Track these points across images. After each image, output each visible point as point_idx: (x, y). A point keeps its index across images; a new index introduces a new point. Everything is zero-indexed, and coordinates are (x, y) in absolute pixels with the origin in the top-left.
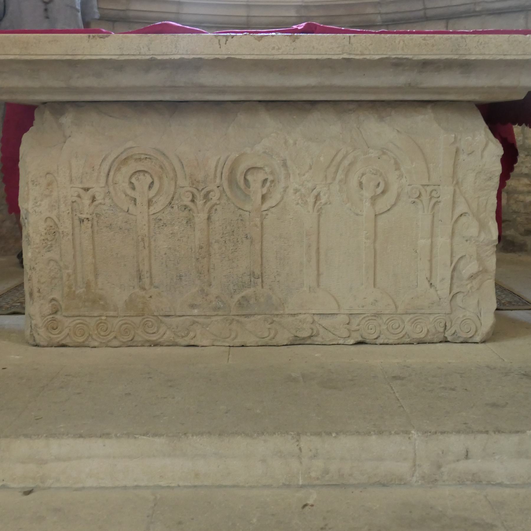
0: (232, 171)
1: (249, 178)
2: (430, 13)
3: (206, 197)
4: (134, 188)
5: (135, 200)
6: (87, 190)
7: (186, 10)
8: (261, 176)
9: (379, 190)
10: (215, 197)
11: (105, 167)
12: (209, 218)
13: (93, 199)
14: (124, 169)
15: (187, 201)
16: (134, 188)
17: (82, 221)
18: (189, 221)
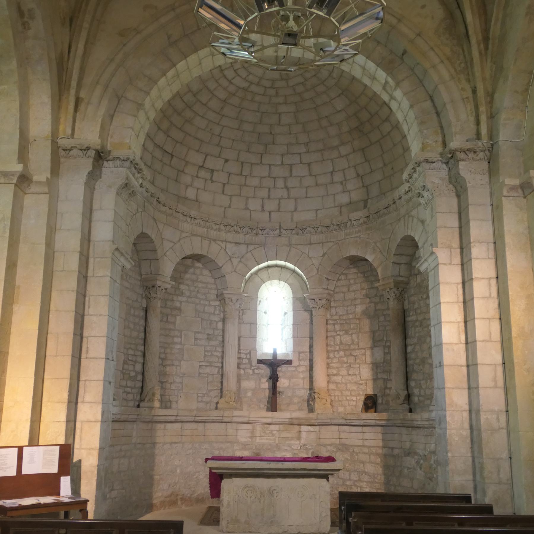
0: (269, 490)
1: (273, 492)
2: (333, 423)
3: (264, 496)
4: (247, 494)
5: (247, 497)
6: (237, 494)
7: (251, 419)
8: (276, 492)
9: (302, 495)
10: (265, 496)
11: (242, 488)
12: (264, 501)
13: (238, 496)
14: (246, 489)
15: (259, 497)
16: (247, 494)
17: (235, 501)
18: (260, 502)
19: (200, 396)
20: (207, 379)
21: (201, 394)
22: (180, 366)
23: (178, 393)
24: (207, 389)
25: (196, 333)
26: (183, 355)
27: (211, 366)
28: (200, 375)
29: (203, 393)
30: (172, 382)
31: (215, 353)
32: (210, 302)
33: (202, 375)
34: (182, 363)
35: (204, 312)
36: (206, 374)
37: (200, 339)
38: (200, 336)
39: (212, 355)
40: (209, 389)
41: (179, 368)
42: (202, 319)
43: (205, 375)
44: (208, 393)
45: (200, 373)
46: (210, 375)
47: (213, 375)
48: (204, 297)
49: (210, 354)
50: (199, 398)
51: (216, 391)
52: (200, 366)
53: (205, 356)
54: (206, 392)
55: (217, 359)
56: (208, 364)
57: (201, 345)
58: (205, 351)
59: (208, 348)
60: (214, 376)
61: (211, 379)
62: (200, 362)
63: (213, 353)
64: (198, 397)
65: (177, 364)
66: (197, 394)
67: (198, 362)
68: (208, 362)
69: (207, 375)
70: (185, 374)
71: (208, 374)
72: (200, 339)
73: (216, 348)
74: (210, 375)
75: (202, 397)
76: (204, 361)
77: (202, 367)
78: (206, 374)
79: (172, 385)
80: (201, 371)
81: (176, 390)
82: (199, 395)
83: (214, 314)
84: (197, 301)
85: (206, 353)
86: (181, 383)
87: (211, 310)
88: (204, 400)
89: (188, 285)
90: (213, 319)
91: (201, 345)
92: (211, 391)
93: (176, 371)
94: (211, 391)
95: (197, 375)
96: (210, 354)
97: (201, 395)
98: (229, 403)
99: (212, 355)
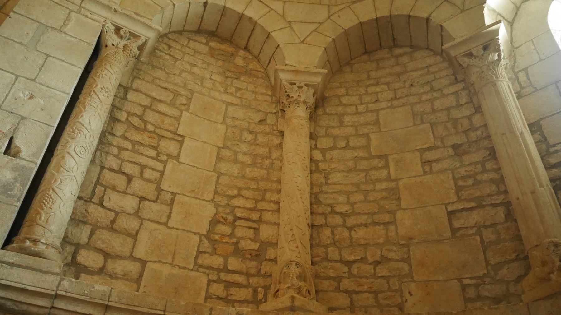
19: (470, 285)
20: (478, 238)
21: (471, 278)
22: (394, 223)
23: (400, 285)
24: (487, 262)
25: (423, 151)
26: (399, 199)
27: (479, 206)
28: (458, 234)
29: (474, 275)
30: (379, 259)
31: (485, 177)
32: (442, 91)
33: (461, 232)
34: (399, 215)
35: (434, 111)
36: (472, 228)
37: (437, 161)
38: (431, 155)
39: (477, 183)
40: (492, 262)
41: (392, 228)
42: (432, 125)
43: (473, 231)
44: (492, 272)
45: (454, 231)
46: (486, 227)
47: (493, 225)
48: (427, 88)
49: (470, 182)
50: (467, 290)
51: (516, 264)
52: (451, 214)
53: (459, 189)
54: (485, 272)
55: (494, 187)
56: (473, 204)
57: (441, 171)
58: (455, 180)
59: (463, 172)
60: (499, 227)
61: (493, 237)
62: (447, 205)
63: (479, 177)
64: (464, 288)
65: (387, 220)
66: (459, 280)
67: (443, 207)
68: (470, 200)
69: (475, 229)
70: (411, 239)
71: (480, 228)
72: (437, 161)
73: (483, 166)
74: (486, 227)
75: (477, 286)
76: (460, 200)
77: (459, 215)
78: (472, 228)
79: (380, 266)
80: (456, 224)
81: (394, 276)
82: (467, 282)
83: (459, 106)
84: (413, 99)
85: (460, 183)
86: (407, 260)
87: (451, 101)
88: (486, 294)
89: (388, 84)
90: (460, 116)
91: (441, 171)
92: (500, 265)
93: (387, 235)
94: (500, 265)
95: (449, 234)
96: (470, 182)
97: (473, 282)
98: (550, 280)
99: (477, 183)
